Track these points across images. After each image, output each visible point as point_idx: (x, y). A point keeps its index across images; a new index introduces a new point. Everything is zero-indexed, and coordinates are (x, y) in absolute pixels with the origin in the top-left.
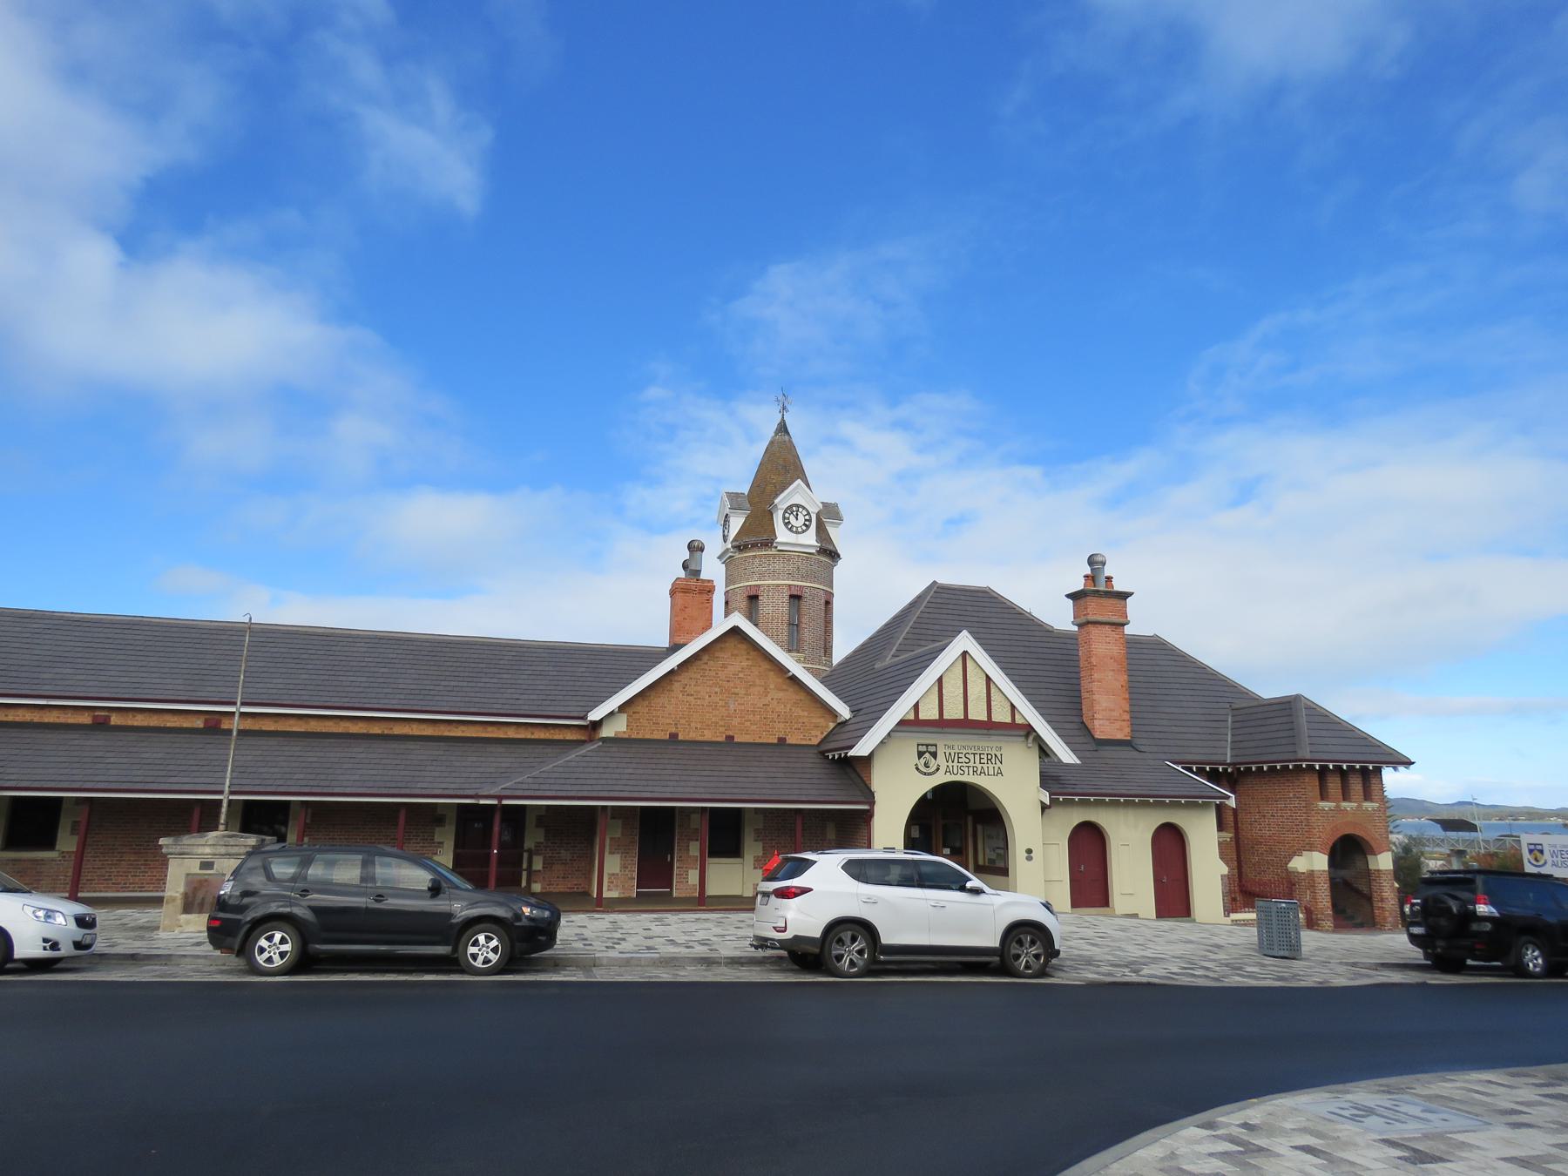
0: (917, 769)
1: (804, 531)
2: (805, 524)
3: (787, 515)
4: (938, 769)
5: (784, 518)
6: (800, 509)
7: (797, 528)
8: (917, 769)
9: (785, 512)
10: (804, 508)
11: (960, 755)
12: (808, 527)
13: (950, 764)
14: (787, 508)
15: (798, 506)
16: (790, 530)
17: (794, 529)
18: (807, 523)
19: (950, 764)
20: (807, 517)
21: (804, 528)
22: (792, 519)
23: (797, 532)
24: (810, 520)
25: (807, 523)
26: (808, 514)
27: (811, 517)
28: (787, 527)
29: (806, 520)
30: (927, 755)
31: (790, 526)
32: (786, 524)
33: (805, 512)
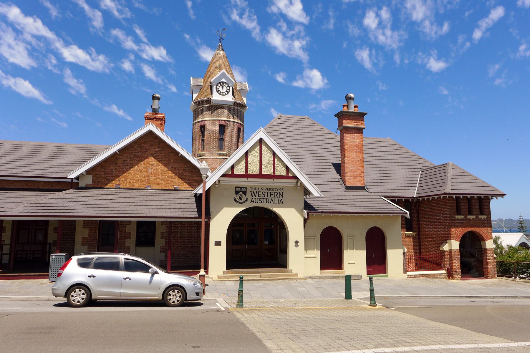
1: (226, 94)
2: (227, 91)
4: (247, 200)
5: (216, 88)
6: (225, 84)
12: (228, 92)
13: (254, 197)
16: (220, 94)
18: (228, 91)
19: (254, 197)
20: (228, 88)
21: (226, 93)
24: (229, 89)
28: (218, 93)
29: (227, 89)
30: (241, 193)
31: (219, 92)
32: (218, 91)
33: (227, 86)
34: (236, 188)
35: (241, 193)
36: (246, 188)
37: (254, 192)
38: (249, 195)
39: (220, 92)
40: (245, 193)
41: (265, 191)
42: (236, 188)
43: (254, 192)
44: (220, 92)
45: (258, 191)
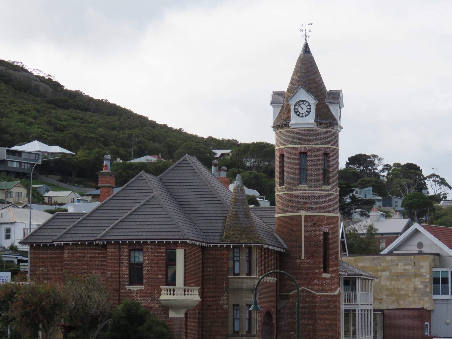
1: (306, 115)
2: (307, 111)
7: (302, 114)
9: (295, 105)
10: (306, 102)
12: (309, 112)
14: (297, 103)
15: (303, 101)
17: (304, 115)
18: (309, 110)
20: (309, 107)
21: (307, 113)
22: (300, 110)
23: (303, 116)
24: (310, 109)
25: (309, 110)
26: (309, 105)
27: (310, 107)
29: (308, 109)
32: (296, 112)
33: (307, 104)
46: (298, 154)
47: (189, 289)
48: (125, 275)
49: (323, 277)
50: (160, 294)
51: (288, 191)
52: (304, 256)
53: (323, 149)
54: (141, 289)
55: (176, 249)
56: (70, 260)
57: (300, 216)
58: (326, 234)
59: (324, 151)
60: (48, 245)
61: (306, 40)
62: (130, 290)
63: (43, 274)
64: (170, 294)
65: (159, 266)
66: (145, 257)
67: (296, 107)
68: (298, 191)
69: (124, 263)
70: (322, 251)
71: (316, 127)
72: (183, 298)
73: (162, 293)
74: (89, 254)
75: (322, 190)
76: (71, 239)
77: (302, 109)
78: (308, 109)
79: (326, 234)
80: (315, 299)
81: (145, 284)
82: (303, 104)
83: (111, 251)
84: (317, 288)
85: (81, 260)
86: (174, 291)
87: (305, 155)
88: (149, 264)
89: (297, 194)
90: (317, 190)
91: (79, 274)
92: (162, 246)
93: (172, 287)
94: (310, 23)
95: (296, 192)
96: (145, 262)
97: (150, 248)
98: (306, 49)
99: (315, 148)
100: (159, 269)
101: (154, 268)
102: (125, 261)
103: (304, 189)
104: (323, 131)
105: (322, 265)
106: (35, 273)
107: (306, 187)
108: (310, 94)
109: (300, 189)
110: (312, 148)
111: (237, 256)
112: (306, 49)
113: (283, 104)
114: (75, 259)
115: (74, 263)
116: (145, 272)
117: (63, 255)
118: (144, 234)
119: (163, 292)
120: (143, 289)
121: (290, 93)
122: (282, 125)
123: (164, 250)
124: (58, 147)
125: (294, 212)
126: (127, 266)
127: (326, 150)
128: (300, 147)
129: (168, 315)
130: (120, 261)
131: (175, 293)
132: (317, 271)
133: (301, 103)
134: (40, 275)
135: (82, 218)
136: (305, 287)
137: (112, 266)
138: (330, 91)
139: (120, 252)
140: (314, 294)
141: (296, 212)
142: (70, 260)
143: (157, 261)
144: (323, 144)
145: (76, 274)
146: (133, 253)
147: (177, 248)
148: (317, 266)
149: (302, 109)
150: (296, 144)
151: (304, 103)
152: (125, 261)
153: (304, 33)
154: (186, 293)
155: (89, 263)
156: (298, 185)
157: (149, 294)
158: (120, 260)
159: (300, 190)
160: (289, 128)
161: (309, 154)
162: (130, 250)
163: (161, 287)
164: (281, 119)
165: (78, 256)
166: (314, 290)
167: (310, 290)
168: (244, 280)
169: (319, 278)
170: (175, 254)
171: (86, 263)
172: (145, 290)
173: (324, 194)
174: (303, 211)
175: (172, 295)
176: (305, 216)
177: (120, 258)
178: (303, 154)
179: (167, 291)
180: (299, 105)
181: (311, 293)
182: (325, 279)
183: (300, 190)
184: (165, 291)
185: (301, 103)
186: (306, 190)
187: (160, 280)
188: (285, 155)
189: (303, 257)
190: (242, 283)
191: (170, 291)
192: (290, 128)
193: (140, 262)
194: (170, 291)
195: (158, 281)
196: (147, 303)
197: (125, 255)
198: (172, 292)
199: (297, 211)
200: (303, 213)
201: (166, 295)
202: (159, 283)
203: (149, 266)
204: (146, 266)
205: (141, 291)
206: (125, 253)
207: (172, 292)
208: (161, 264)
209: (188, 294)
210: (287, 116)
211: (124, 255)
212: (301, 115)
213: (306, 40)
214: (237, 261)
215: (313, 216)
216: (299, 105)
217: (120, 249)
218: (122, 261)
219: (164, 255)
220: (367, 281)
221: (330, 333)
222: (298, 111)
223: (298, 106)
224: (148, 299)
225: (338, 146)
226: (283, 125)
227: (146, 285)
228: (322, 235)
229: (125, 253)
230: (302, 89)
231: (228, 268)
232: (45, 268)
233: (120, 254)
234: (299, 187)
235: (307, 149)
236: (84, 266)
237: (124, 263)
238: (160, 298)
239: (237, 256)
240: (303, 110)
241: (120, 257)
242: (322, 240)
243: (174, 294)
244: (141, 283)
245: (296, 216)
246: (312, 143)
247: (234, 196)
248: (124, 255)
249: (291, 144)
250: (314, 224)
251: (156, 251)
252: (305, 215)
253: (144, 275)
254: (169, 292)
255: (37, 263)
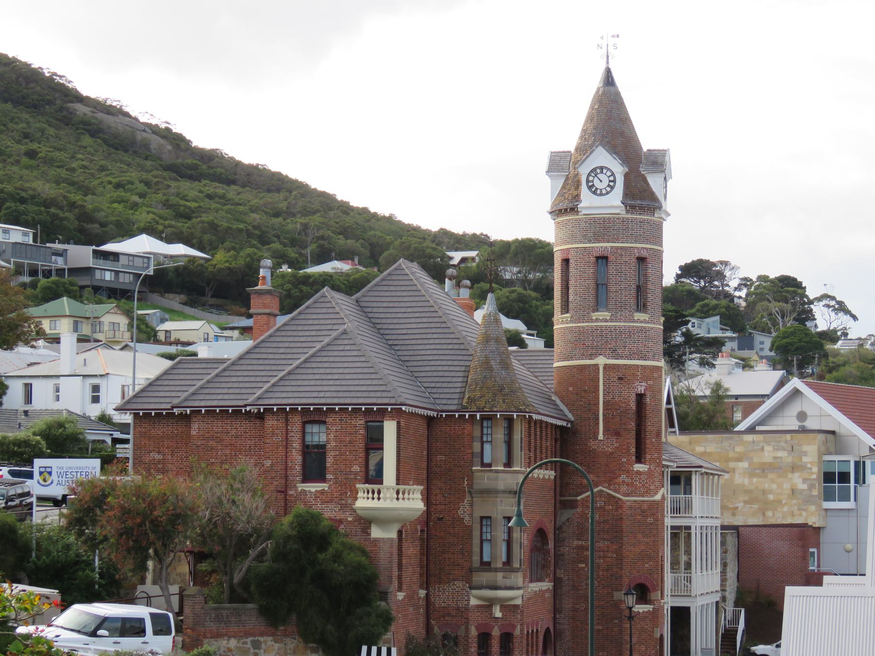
0: (39, 482)
1: (608, 193)
2: (609, 186)
3: (591, 178)
4: (52, 483)
7: (601, 190)
8: (39, 482)
9: (589, 175)
10: (608, 169)
11: (67, 473)
12: (612, 188)
13: (60, 479)
14: (592, 171)
15: (602, 168)
16: (594, 193)
18: (612, 184)
19: (60, 479)
20: (612, 178)
21: (609, 189)
22: (597, 183)
23: (601, 194)
24: (614, 181)
25: (612, 184)
26: (613, 174)
27: (615, 178)
30: (45, 474)
31: (593, 190)
32: (590, 188)
33: (609, 173)
34: (40, 467)
35: (45, 474)
36: (51, 467)
37: (60, 472)
38: (54, 476)
39: (595, 188)
40: (50, 473)
41: (74, 471)
42: (40, 467)
43: (60, 472)
44: (595, 188)
45: (65, 470)
46: (593, 259)
47: (405, 489)
48: (296, 464)
49: (635, 470)
50: (356, 499)
51: (576, 323)
52: (603, 434)
53: (636, 250)
54: (324, 490)
55: (383, 422)
56: (201, 440)
57: (596, 366)
58: (640, 397)
59: (637, 254)
60: (164, 413)
61: (608, 63)
62: (304, 490)
63: (156, 464)
64: (373, 498)
65: (353, 451)
66: (330, 434)
67: (591, 178)
68: (592, 322)
69: (294, 445)
70: (633, 425)
71: (624, 212)
72: (395, 504)
73: (358, 496)
74: (235, 428)
75: (634, 321)
76: (203, 404)
77: (601, 181)
78: (610, 181)
79: (640, 397)
80: (621, 507)
81: (330, 481)
82: (602, 172)
83: (273, 425)
84: (624, 488)
85: (221, 440)
86: (379, 492)
87: (604, 261)
88: (338, 446)
89: (592, 327)
90: (625, 322)
91: (217, 463)
92: (359, 415)
93: (376, 487)
94: (616, 33)
95: (590, 324)
96: (330, 443)
97: (339, 420)
98: (609, 80)
99: (621, 248)
100: (353, 455)
101: (346, 453)
102: (296, 441)
103: (603, 319)
104: (636, 219)
105: (634, 450)
106: (142, 461)
107: (606, 315)
108: (614, 156)
109: (597, 319)
110: (617, 248)
111: (487, 434)
112: (609, 80)
113: (567, 173)
114: (210, 438)
115: (208, 444)
116: (329, 461)
117: (190, 431)
118: (328, 395)
119: (360, 494)
120: (326, 489)
121: (580, 155)
122: (566, 210)
123: (362, 422)
124: (181, 245)
125: (586, 359)
126: (299, 450)
127: (642, 252)
128: (597, 247)
129: (369, 534)
130: (287, 441)
131: (381, 496)
132: (624, 460)
133: (598, 171)
134: (150, 464)
135: (222, 367)
136: (604, 487)
137: (274, 450)
138: (648, 150)
139: (287, 425)
140: (619, 499)
141: (589, 359)
142: (201, 440)
143: (350, 442)
144: (636, 242)
145: (212, 463)
146: (309, 428)
147: (386, 420)
148: (624, 451)
149: (601, 181)
150: (590, 242)
151: (605, 171)
152: (296, 441)
153: (604, 51)
154: (401, 496)
155: (233, 444)
156: (594, 312)
157: (337, 497)
158: (287, 439)
159: (597, 320)
160: (577, 215)
161: (612, 258)
162: (304, 423)
163: (358, 486)
164: (565, 199)
165: (216, 433)
166: (618, 492)
167: (613, 491)
168: (500, 475)
169: (628, 472)
170: (381, 430)
171: (230, 444)
172: (330, 491)
173: (637, 327)
174: (601, 356)
175: (376, 500)
176: (606, 365)
177: (287, 436)
178: (602, 259)
179: (368, 492)
180: (596, 175)
181: (614, 497)
182: (638, 473)
183: (597, 320)
184: (364, 493)
185: (598, 171)
186: (606, 321)
187: (356, 473)
188: (571, 261)
189: (601, 436)
190: (497, 479)
191: (373, 492)
192: (580, 214)
193: (321, 443)
194: (373, 492)
195: (352, 477)
196: (334, 512)
197: (297, 432)
198: (376, 495)
199: (591, 356)
200: (601, 361)
201: (366, 499)
202: (354, 479)
203: (337, 451)
204: (331, 451)
205: (322, 492)
206: (296, 427)
207: (376, 495)
208: (358, 446)
209: (403, 499)
210: (575, 193)
211: (293, 432)
212: (598, 192)
213: (608, 63)
214: (487, 442)
215: (619, 365)
216: (596, 175)
217: (287, 420)
218: (292, 441)
219: (362, 432)
220: (711, 477)
221: (647, 565)
222: (593, 185)
223: (594, 177)
224: (334, 507)
225: (661, 245)
226: (567, 209)
227: (331, 483)
228: (633, 398)
229: (296, 427)
230: (600, 148)
231: (472, 453)
232: (159, 452)
233: (287, 429)
234: (595, 315)
235: (609, 250)
236: (226, 449)
237: (294, 445)
238: (355, 505)
239: (487, 434)
240: (602, 182)
241: (287, 434)
242: (634, 408)
243: (379, 499)
244: (322, 479)
245: (589, 366)
246: (617, 240)
247: (484, 331)
248: (293, 432)
249: (581, 242)
250: (620, 379)
251: (349, 424)
252: (605, 364)
253: (328, 465)
254: (370, 495)
255: (145, 443)
